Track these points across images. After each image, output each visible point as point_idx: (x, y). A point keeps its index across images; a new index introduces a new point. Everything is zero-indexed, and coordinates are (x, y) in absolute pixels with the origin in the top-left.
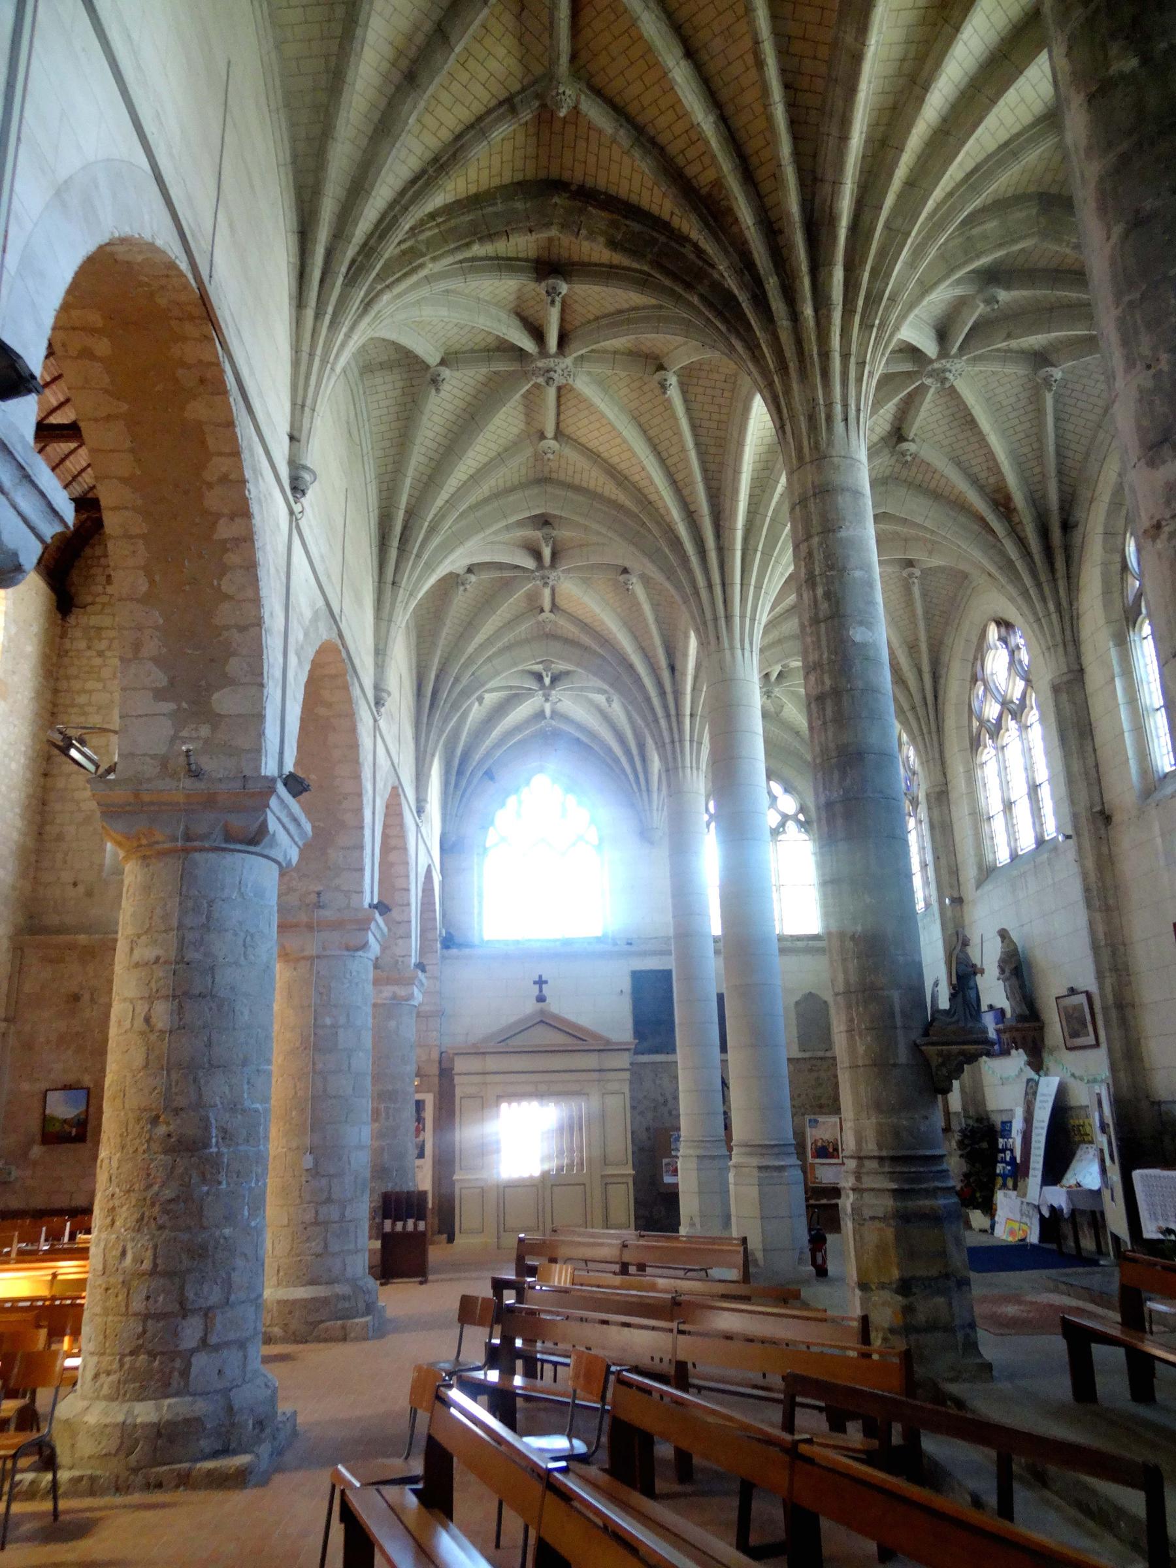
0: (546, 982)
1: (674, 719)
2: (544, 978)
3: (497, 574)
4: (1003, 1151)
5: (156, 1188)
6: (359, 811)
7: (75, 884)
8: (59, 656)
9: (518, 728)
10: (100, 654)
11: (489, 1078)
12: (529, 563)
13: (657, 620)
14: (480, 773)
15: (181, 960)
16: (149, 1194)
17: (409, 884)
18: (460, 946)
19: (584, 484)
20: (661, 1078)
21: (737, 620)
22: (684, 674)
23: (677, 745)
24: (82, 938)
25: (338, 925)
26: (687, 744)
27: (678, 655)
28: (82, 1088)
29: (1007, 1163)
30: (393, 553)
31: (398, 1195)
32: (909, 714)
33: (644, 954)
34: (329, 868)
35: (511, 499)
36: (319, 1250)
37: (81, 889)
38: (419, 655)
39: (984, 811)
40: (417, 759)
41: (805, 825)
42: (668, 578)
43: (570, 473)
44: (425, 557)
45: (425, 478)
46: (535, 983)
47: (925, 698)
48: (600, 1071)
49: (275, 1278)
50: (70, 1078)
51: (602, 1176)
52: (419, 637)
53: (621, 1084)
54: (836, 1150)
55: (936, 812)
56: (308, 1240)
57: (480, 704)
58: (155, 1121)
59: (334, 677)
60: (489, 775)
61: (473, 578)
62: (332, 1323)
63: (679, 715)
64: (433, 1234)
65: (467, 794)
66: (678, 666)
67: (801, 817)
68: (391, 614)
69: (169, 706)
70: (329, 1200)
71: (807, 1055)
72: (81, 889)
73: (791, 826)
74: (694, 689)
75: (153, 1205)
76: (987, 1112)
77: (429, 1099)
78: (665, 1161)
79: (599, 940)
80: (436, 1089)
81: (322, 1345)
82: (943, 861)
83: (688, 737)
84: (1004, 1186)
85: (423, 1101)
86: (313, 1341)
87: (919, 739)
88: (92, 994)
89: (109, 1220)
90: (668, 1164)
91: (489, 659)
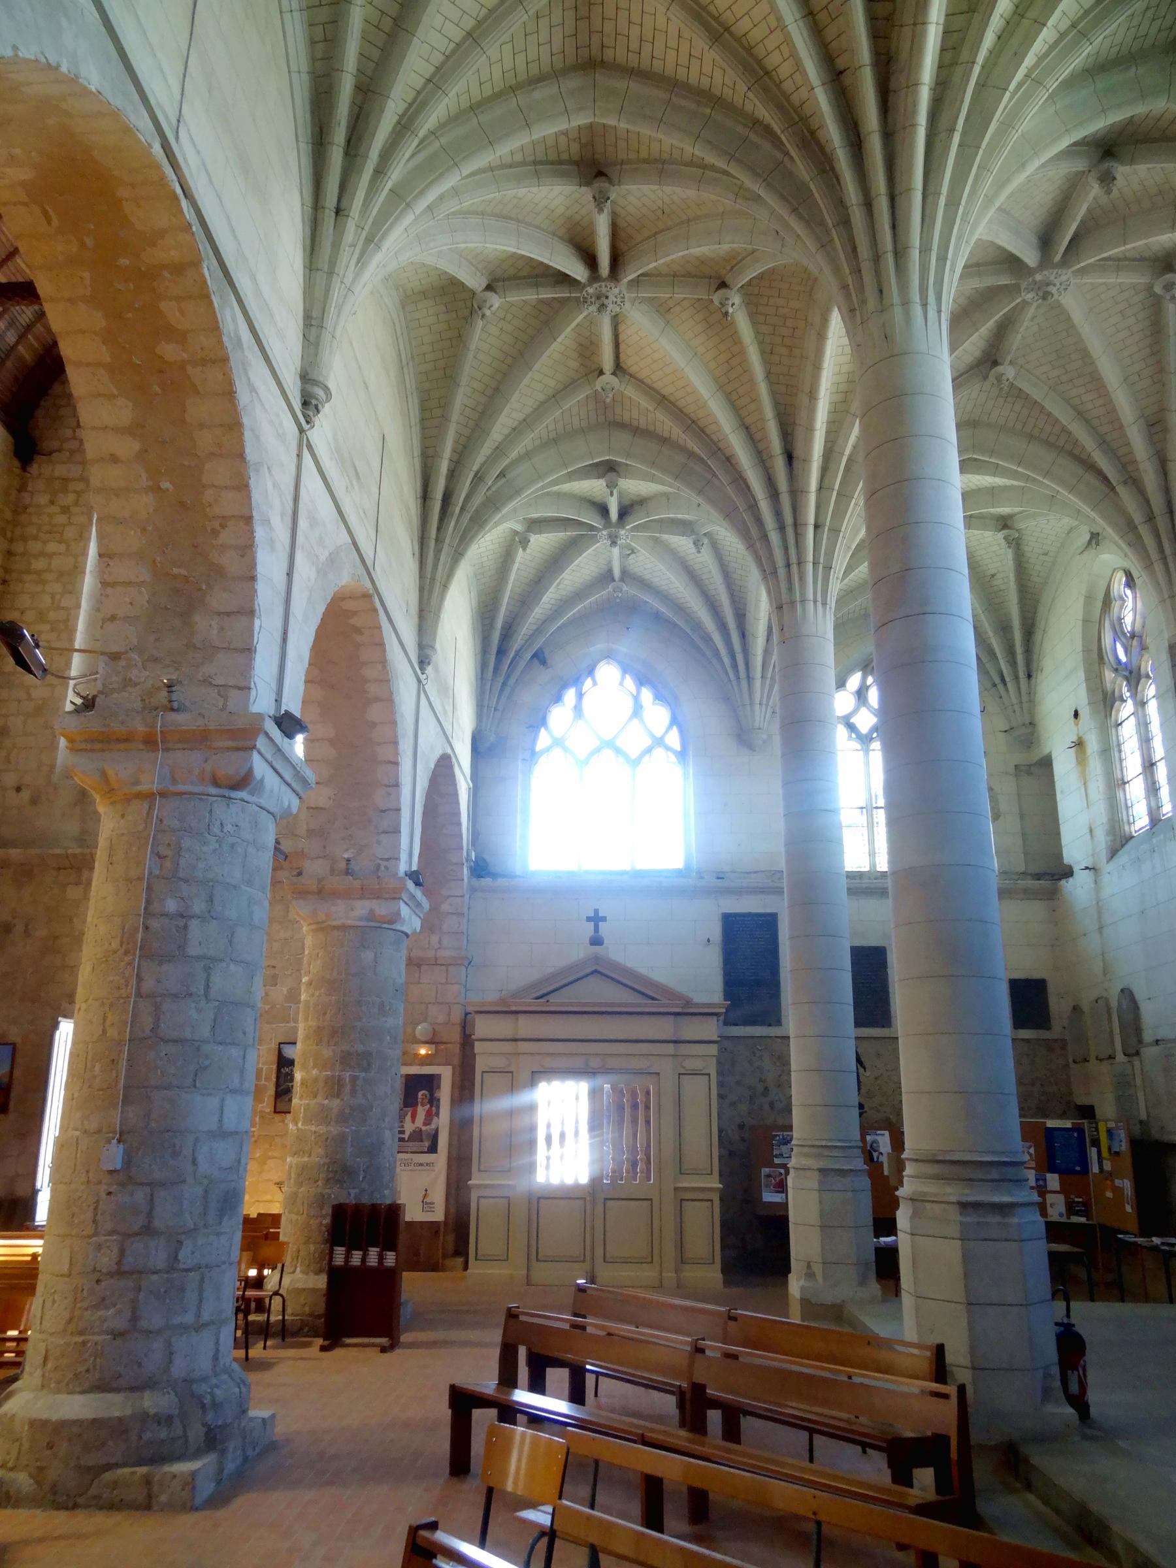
0: (604, 919)
1: (790, 531)
2: (601, 914)
3: (531, 296)
6: (247, 549)
7: (18, 789)
8: (15, 512)
9: (578, 595)
10: (65, 510)
11: (523, 1047)
12: (578, 271)
13: (768, 374)
14: (528, 656)
17: (396, 753)
18: (494, 876)
19: (658, 66)
20: (761, 1058)
21: (915, 254)
22: (807, 460)
23: (794, 569)
24: (15, 853)
25: (199, 739)
26: (810, 567)
27: (799, 432)
28: (7, 1044)
30: (336, 156)
31: (358, 1208)
32: (1144, 530)
33: (739, 892)
34: (194, 646)
35: (538, 95)
36: (122, 1324)
37: (26, 794)
38: (424, 438)
40: (421, 589)
42: (794, 210)
43: (634, 46)
44: (395, 174)
45: (387, 23)
46: (589, 919)
48: (675, 1042)
49: (39, 1373)
51: (676, 1189)
52: (423, 409)
53: (706, 1058)
56: (102, 1303)
57: (524, 549)
59: (179, 269)
60: (539, 657)
61: (495, 301)
62: (127, 1470)
64: (445, 1256)
65: (512, 680)
66: (798, 452)
68: (333, 264)
70: (148, 1230)
72: (26, 794)
74: (820, 488)
77: (446, 1075)
78: (765, 1171)
79: (679, 873)
80: (456, 1061)
81: (100, 1519)
83: (810, 558)
85: (439, 1076)
86: (87, 1506)
87: (1158, 567)
88: (26, 926)
90: (768, 1176)
91: (527, 455)
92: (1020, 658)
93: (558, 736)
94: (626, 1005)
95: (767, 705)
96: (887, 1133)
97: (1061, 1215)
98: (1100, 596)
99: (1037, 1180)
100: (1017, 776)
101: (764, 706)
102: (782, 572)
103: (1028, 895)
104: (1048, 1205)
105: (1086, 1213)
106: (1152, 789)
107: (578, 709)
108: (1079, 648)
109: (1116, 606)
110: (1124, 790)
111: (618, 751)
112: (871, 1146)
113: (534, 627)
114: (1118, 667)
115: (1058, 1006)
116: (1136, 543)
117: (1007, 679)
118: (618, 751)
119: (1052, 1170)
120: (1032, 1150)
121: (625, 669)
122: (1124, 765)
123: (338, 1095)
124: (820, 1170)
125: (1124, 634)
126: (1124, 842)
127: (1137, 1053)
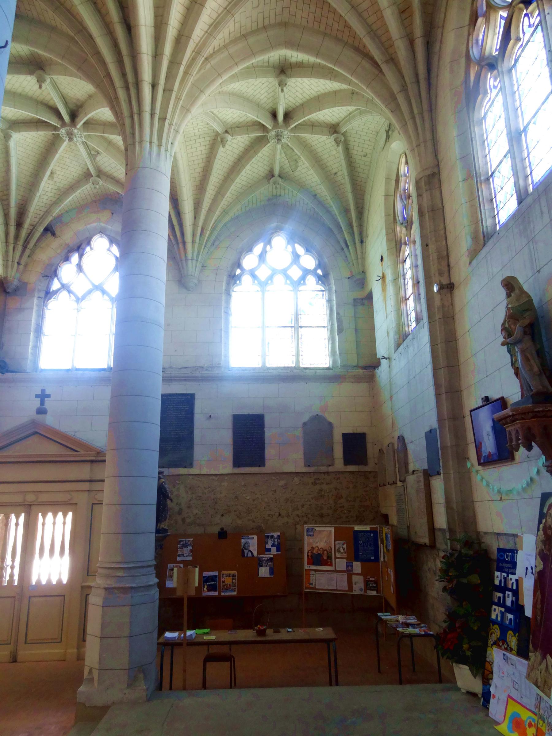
0: (49, 396)
2: (47, 392)
4: (503, 589)
14: (41, 229)
26: (147, 117)
29: (509, 610)
32: (401, 98)
39: (482, 171)
41: (323, 279)
46: (37, 396)
47: (417, 75)
48: (91, 481)
51: (83, 587)
54: (330, 557)
55: (426, 196)
63: (138, 84)
67: (320, 272)
71: (312, 469)
73: (311, 280)
76: (478, 533)
82: (432, 248)
84: (502, 642)
92: (356, 230)
93: (65, 281)
94: (61, 456)
95: (197, 260)
96: (255, 537)
97: (361, 590)
98: (394, 178)
99: (347, 566)
100: (354, 306)
101: (194, 262)
102: (127, 121)
103: (358, 379)
104: (353, 583)
105: (377, 589)
107: (79, 267)
108: (383, 214)
110: (406, 304)
111: (104, 292)
112: (243, 547)
113: (45, 209)
115: (371, 450)
116: (396, 109)
117: (349, 244)
118: (104, 292)
119: (356, 559)
120: (345, 546)
121: (112, 241)
122: (406, 287)
124: (106, 589)
126: (405, 337)
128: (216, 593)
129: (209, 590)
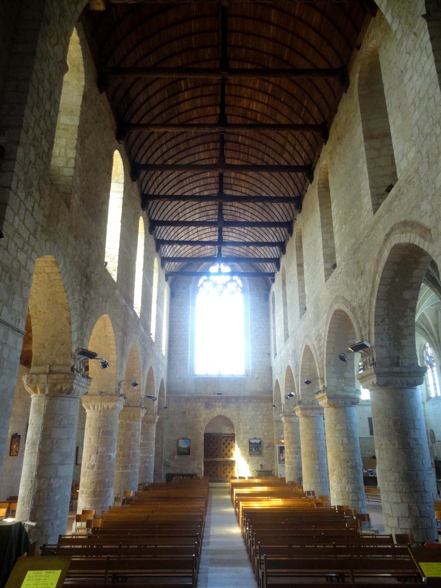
5: (350, 475)
7: (180, 379)
15: (347, 430)
16: (349, 477)
24: (186, 395)
32: (434, 344)
50: (184, 436)
56: (319, 486)
58: (347, 462)
69: (335, 375)
70: (323, 477)
75: (350, 478)
88: (189, 412)
89: (340, 481)
98: (423, 346)
106: (436, 389)
109: (426, 349)
114: (427, 362)
123: (297, 454)
125: (428, 355)
127: (434, 443)
128: (373, 476)
129: (371, 475)
